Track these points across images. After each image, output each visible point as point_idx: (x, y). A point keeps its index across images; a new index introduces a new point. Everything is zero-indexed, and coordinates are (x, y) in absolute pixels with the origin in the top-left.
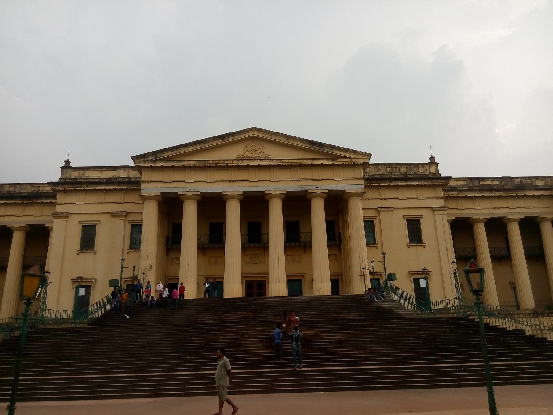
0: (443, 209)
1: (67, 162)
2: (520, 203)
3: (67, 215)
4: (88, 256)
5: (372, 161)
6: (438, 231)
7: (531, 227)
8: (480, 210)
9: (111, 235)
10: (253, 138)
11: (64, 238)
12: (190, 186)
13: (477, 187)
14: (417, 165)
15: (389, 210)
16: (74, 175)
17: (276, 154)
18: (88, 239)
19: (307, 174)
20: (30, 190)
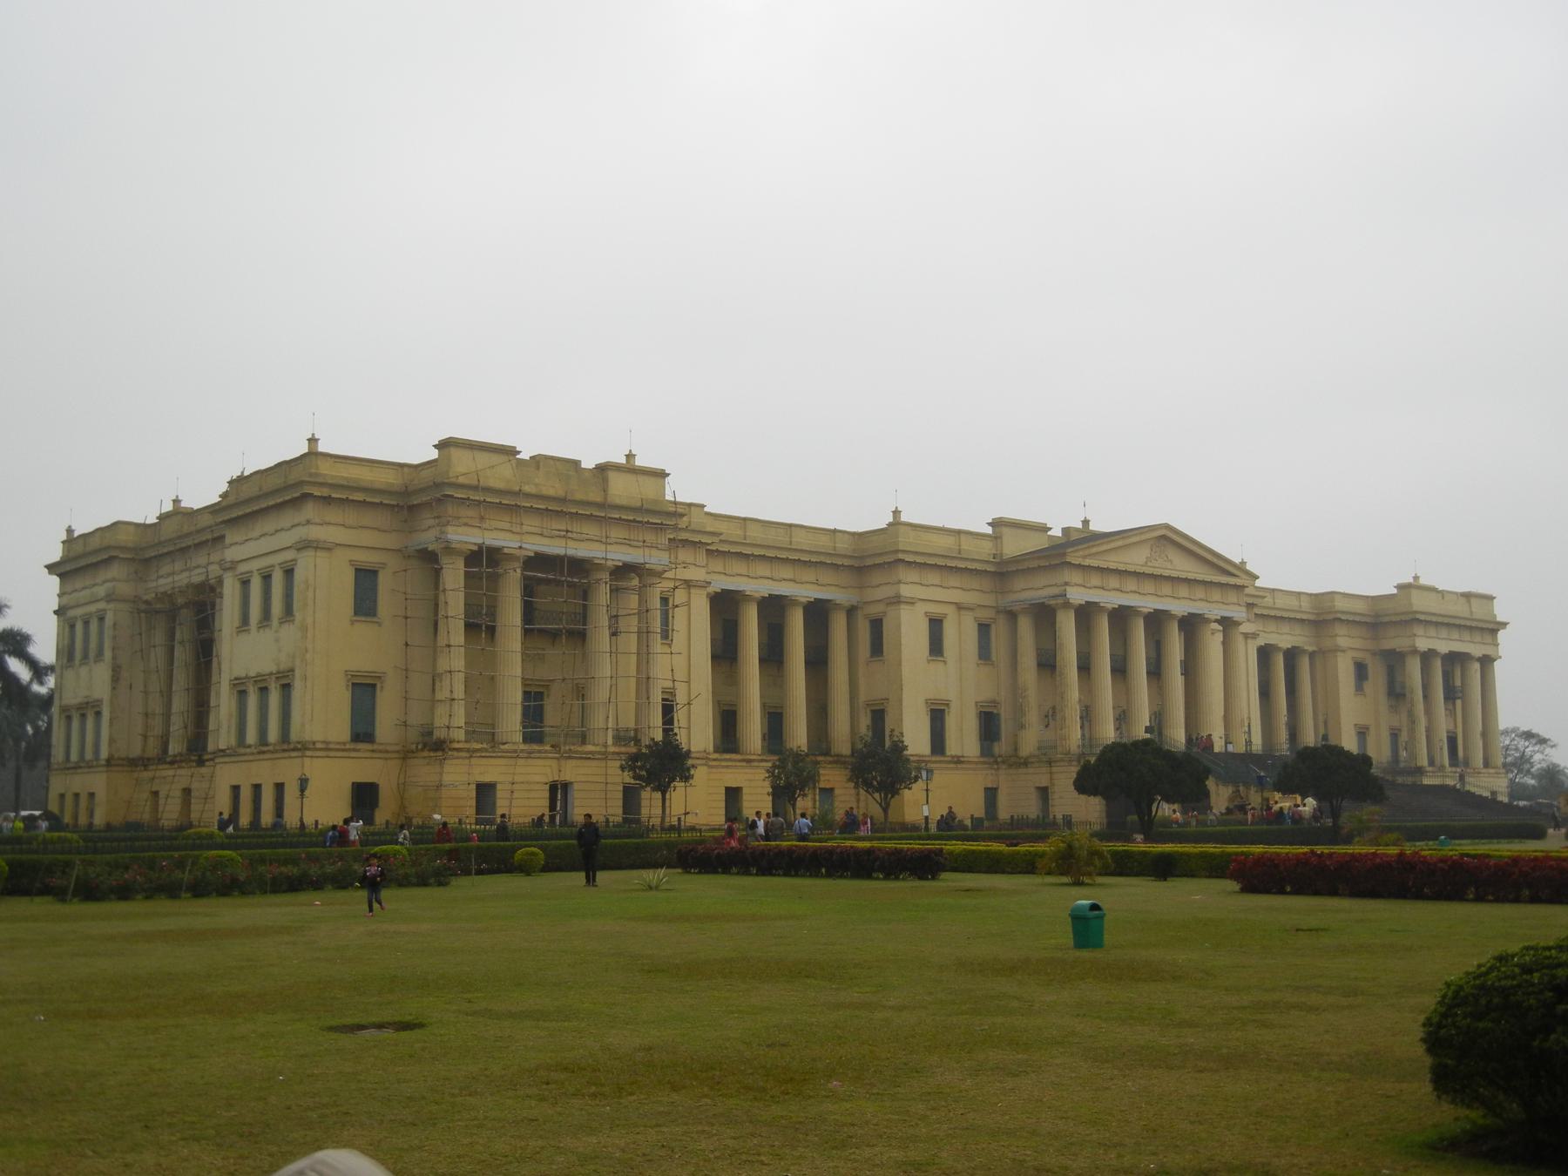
0: (1254, 636)
1: (896, 513)
3: (911, 602)
5: (1258, 583)
9: (960, 636)
10: (1164, 537)
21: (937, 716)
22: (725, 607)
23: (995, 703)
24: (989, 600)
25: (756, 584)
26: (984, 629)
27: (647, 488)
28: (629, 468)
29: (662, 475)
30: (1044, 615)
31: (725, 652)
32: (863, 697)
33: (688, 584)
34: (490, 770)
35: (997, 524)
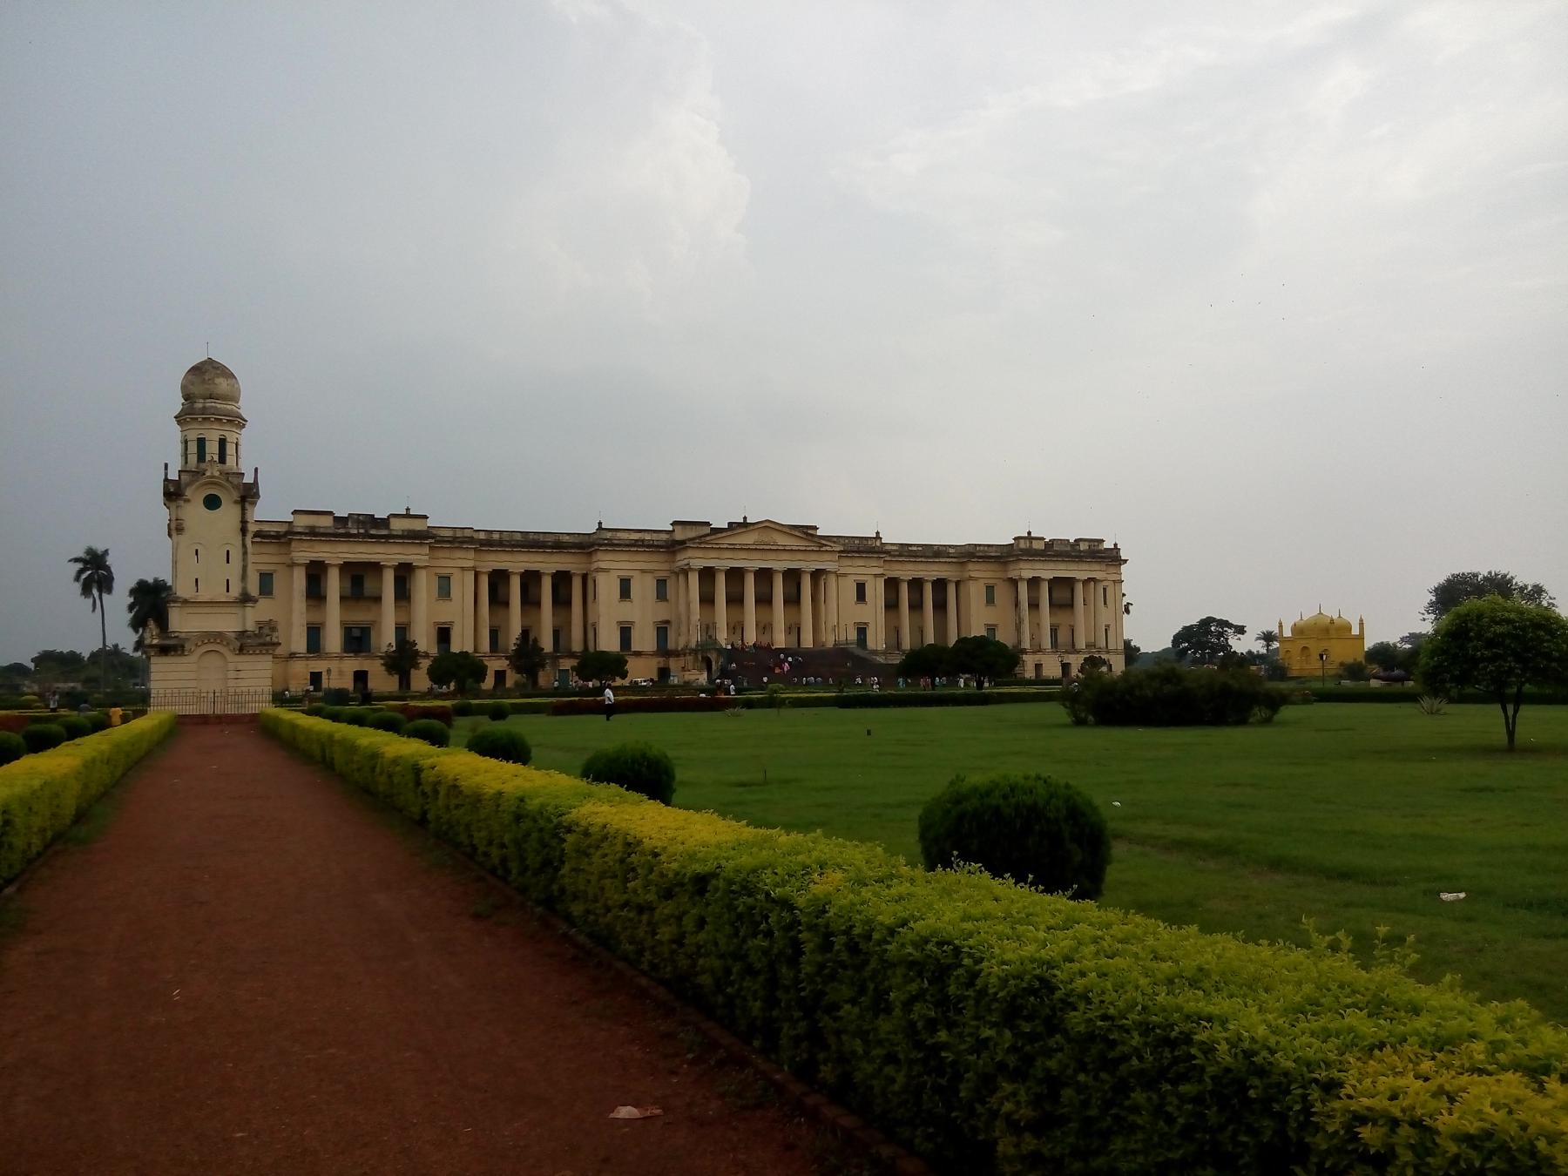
2: (935, 567)
4: (627, 604)
6: (876, 591)
7: (940, 585)
8: (906, 572)
9: (643, 588)
11: (607, 587)
12: (723, 562)
13: (906, 552)
14: (867, 539)
15: (845, 575)
16: (609, 535)
17: (783, 541)
18: (625, 592)
19: (800, 556)
20: (550, 539)
21: (625, 632)
22: (499, 579)
23: (667, 622)
24: (665, 566)
25: (516, 563)
26: (661, 584)
27: (417, 525)
28: (408, 516)
29: (425, 517)
30: (707, 574)
31: (498, 599)
32: (590, 621)
33: (463, 568)
34: (319, 666)
35: (675, 523)
